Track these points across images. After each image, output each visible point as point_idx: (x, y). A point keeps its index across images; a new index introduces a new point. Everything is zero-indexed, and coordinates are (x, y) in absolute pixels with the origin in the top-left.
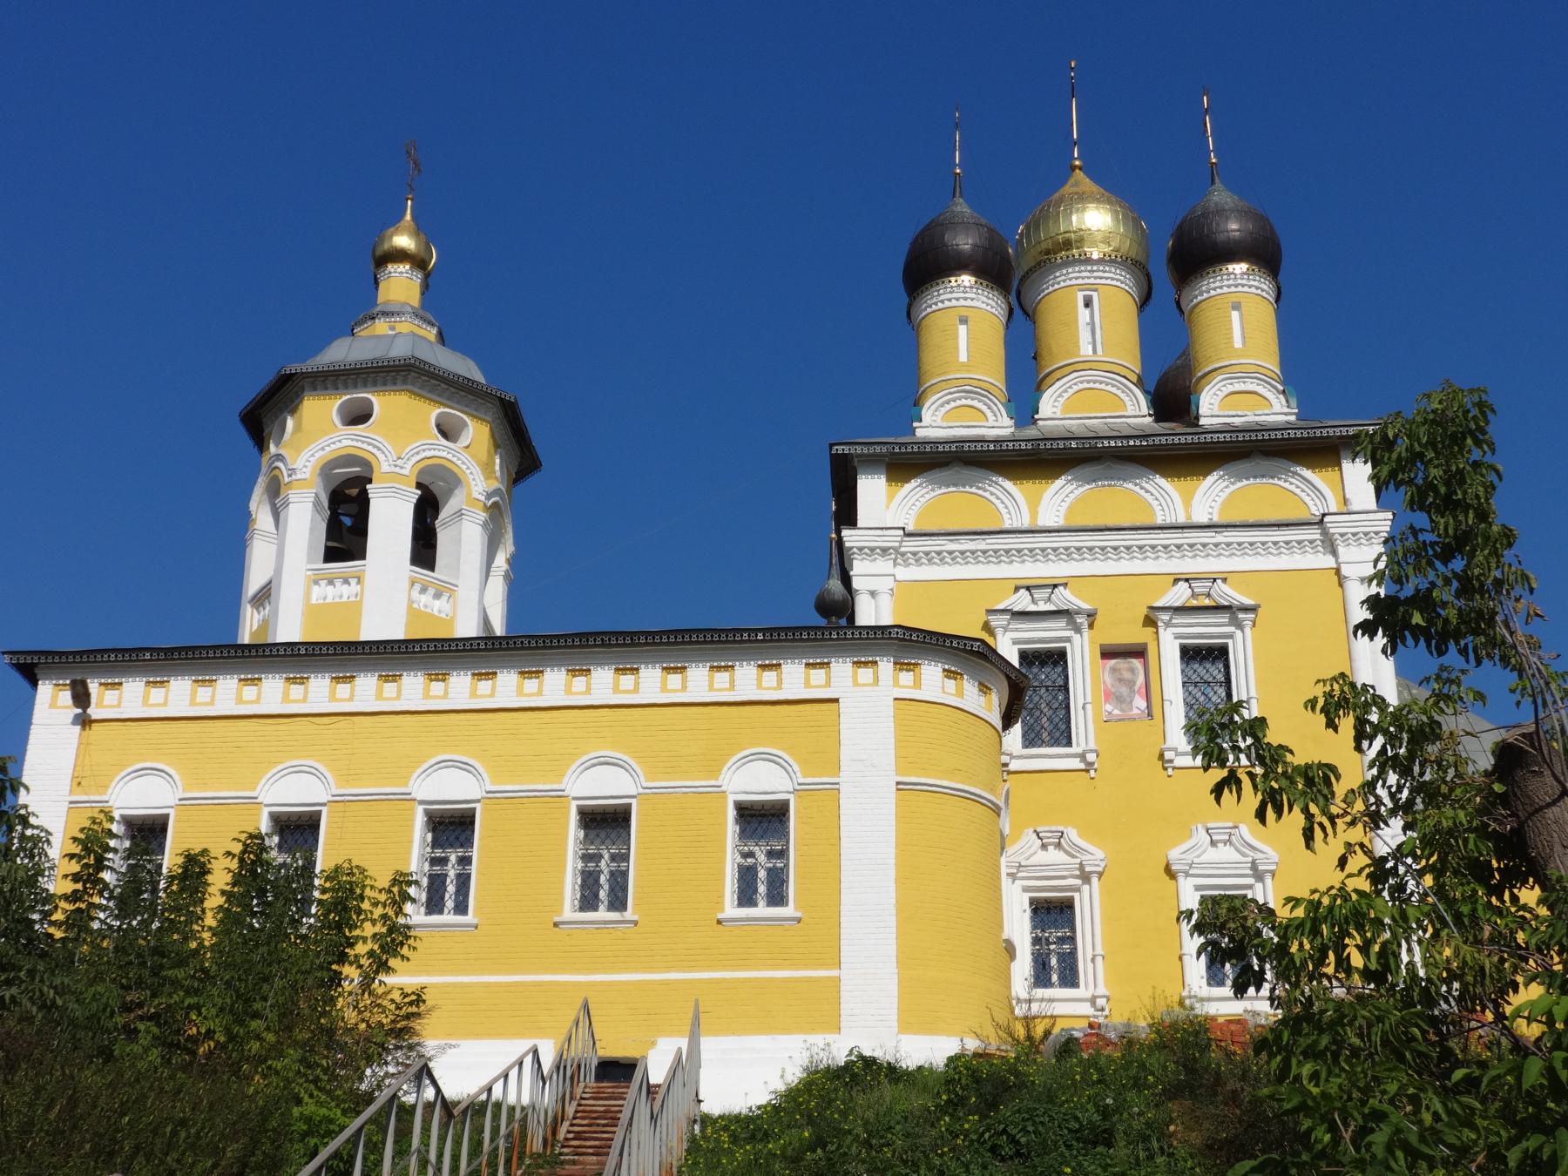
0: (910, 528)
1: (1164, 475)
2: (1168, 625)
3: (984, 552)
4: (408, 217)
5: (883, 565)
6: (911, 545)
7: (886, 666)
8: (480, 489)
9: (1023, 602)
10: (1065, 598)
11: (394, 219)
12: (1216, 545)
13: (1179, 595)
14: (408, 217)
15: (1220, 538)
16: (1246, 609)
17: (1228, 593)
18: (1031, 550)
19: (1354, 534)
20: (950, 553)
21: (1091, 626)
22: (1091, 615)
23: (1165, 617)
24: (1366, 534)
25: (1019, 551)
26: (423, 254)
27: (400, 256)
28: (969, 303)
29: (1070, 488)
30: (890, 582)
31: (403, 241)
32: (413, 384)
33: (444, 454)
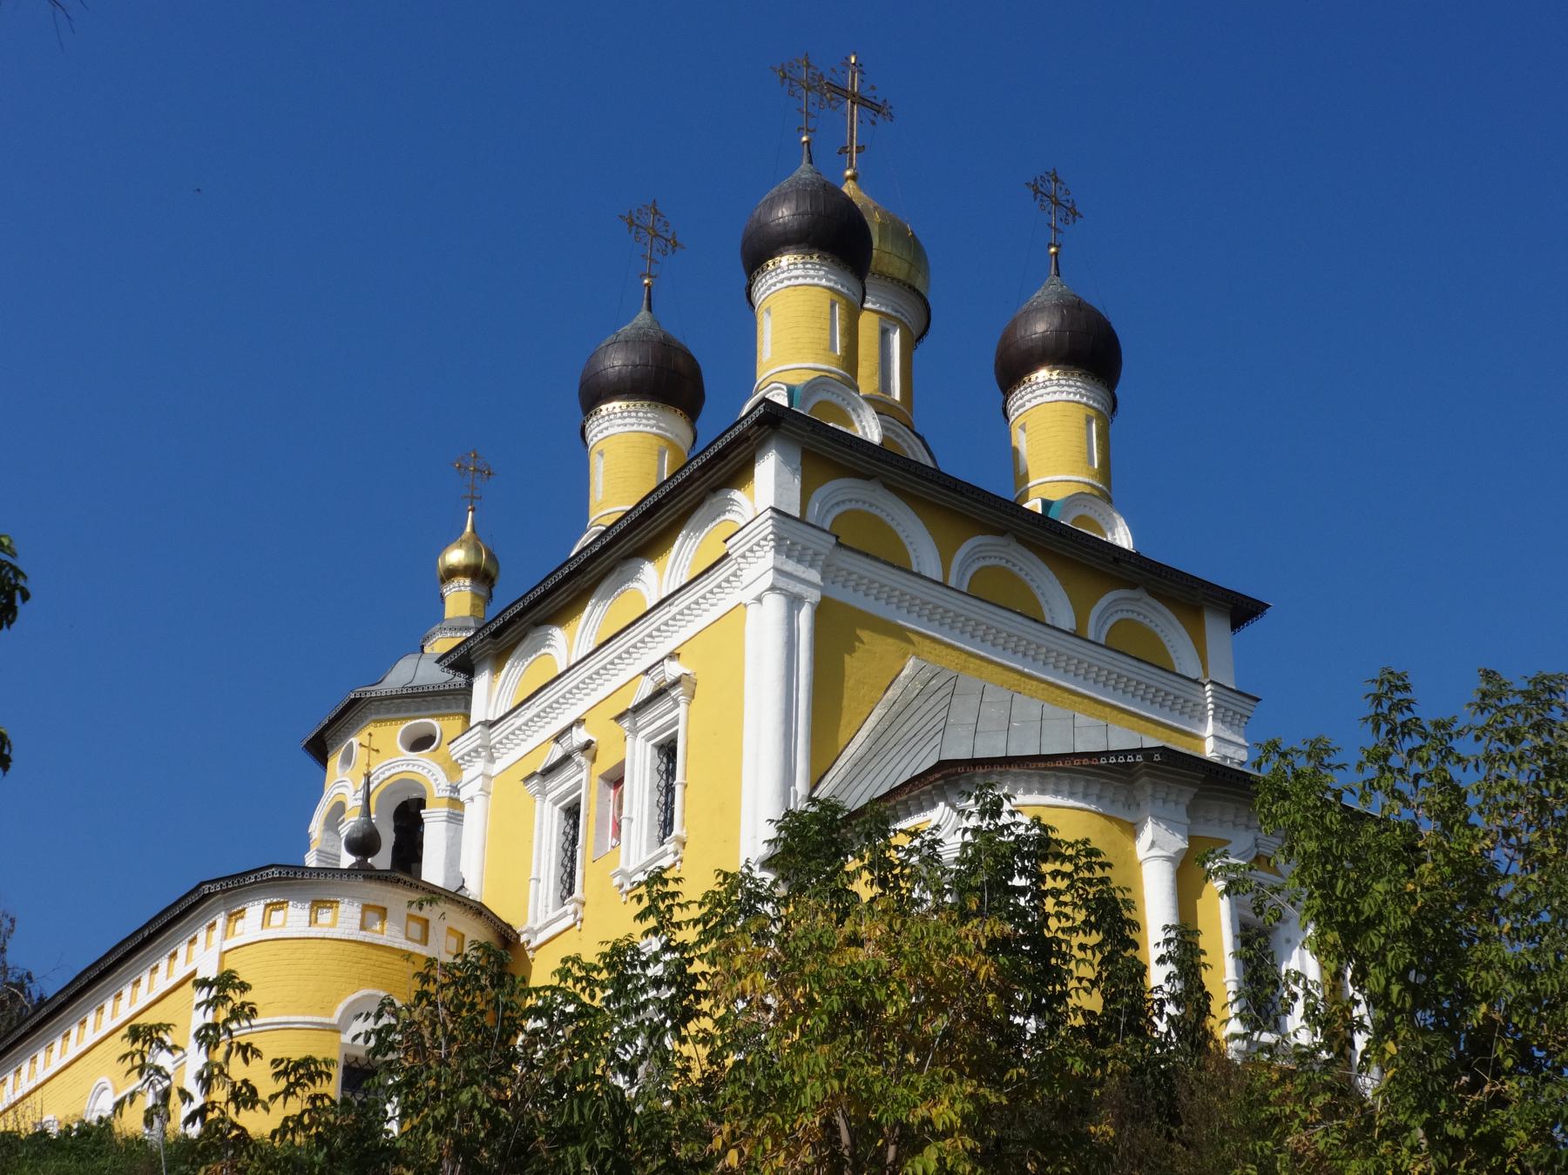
0: (491, 718)
1: (651, 560)
2: (635, 731)
3: (538, 716)
4: (468, 529)
5: (479, 765)
6: (497, 734)
7: (220, 920)
8: (443, 786)
9: (557, 752)
10: (579, 736)
11: (451, 537)
12: (674, 619)
13: (646, 688)
14: (468, 529)
15: (674, 610)
16: (676, 683)
17: (673, 670)
18: (564, 697)
19: (751, 550)
20: (519, 729)
21: (594, 760)
22: (588, 745)
23: (626, 723)
24: (758, 544)
25: (557, 702)
26: (472, 560)
27: (452, 573)
28: (606, 433)
29: (598, 610)
30: (479, 782)
31: (456, 556)
32: (378, 713)
33: (404, 768)
